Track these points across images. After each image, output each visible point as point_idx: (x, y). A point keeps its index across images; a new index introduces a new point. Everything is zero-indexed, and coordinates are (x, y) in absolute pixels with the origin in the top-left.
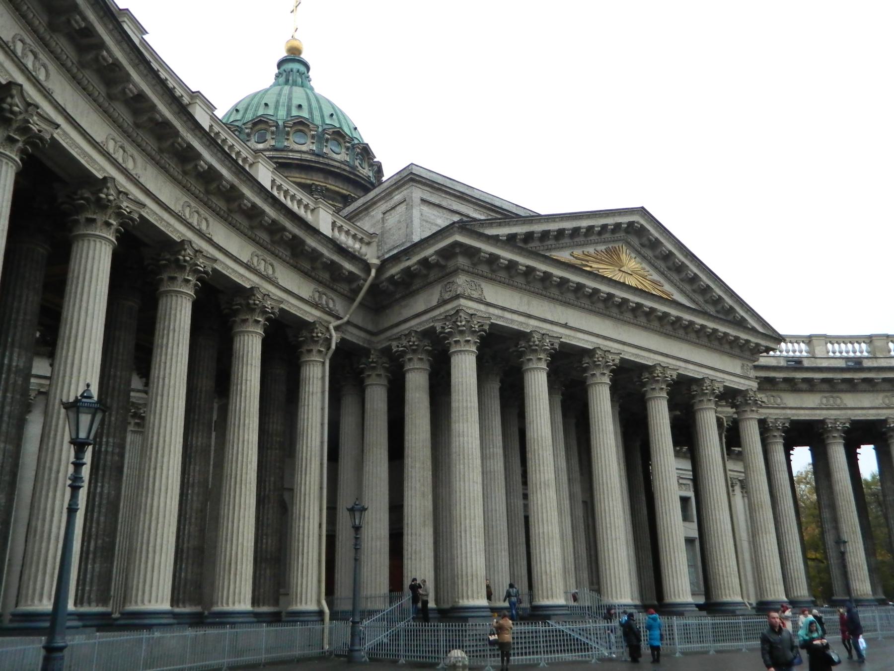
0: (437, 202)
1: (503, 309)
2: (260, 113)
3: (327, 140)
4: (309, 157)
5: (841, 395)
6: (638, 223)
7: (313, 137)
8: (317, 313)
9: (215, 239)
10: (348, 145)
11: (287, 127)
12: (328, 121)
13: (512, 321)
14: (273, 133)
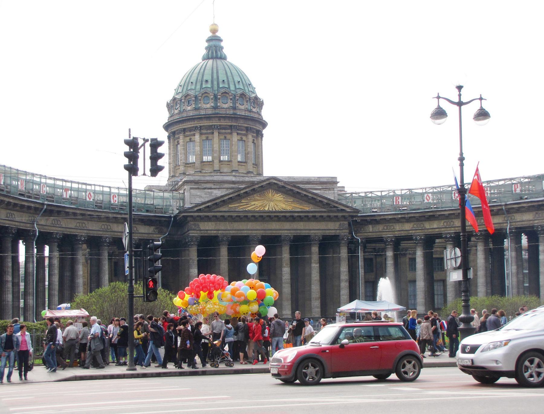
0: (197, 187)
1: (207, 230)
2: (189, 88)
3: (219, 99)
4: (210, 112)
5: (424, 223)
7: (212, 99)
8: (155, 235)
9: (114, 230)
10: (232, 97)
11: (200, 97)
12: (221, 86)
13: (211, 233)
14: (193, 101)
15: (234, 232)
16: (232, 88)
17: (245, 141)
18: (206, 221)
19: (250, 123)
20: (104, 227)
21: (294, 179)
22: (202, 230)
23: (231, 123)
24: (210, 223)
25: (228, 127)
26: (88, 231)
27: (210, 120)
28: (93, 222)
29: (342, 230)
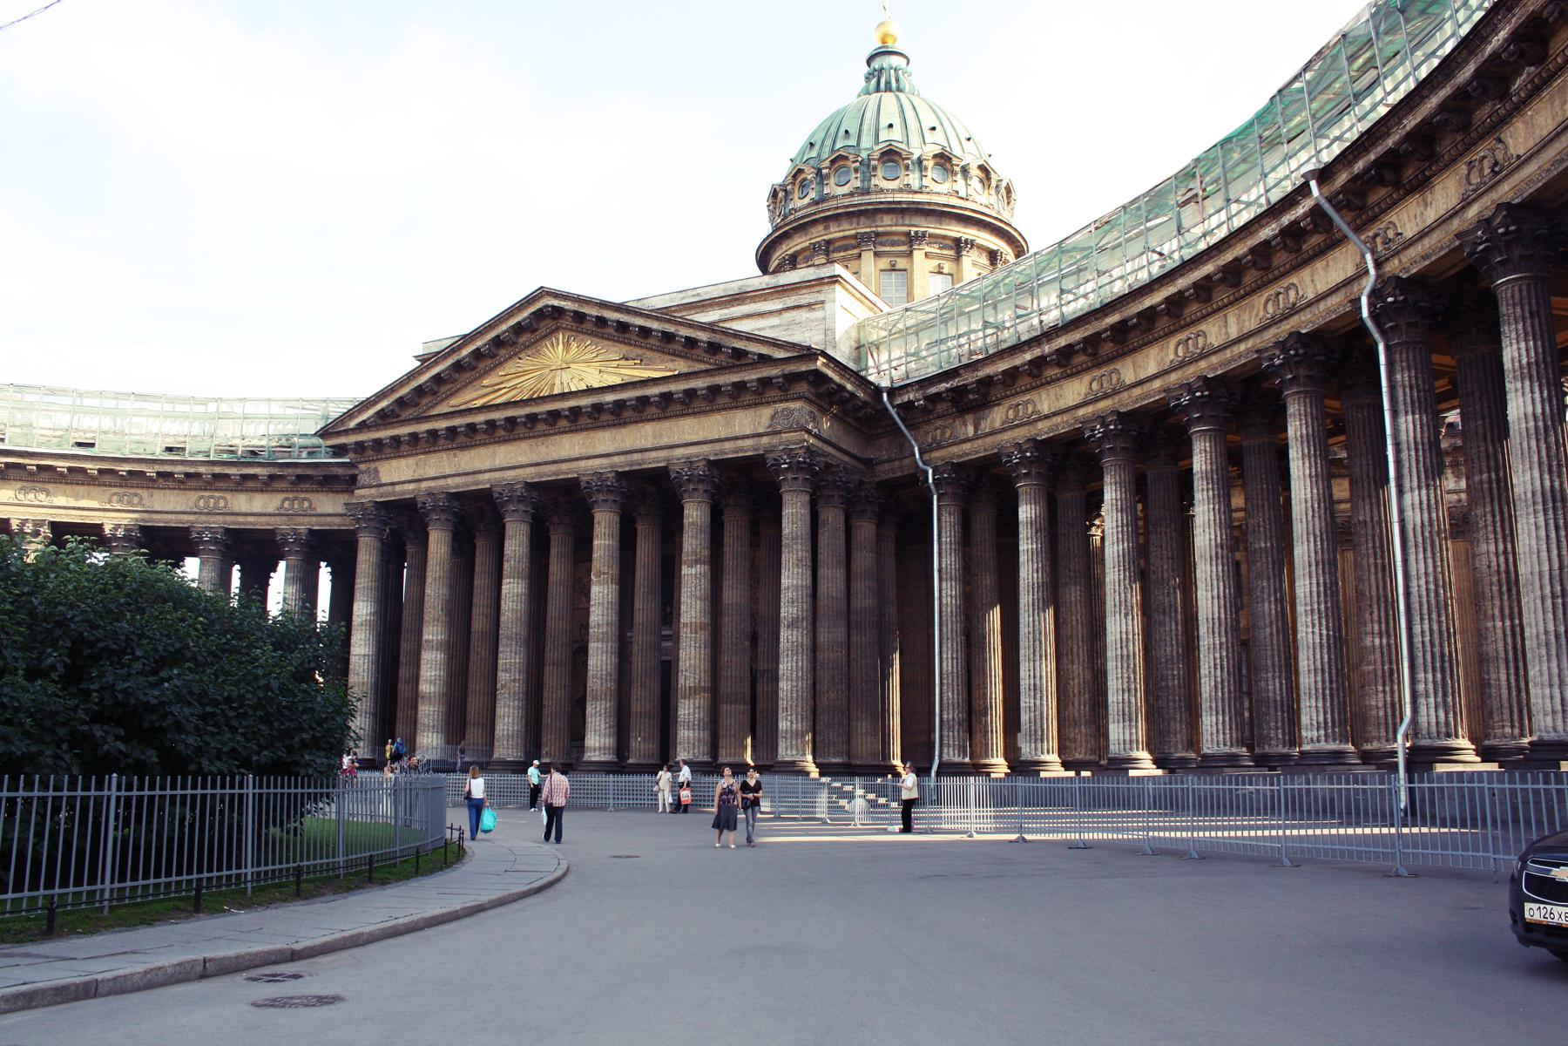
1: (392, 484)
3: (828, 176)
6: (547, 306)
9: (236, 509)
12: (838, 146)
13: (404, 492)
15: (457, 480)
16: (867, 142)
17: (905, 270)
18: (391, 458)
19: (917, 220)
20: (207, 503)
21: (698, 295)
22: (385, 485)
23: (854, 229)
24: (403, 462)
25: (853, 242)
26: (146, 516)
27: (806, 235)
28: (168, 491)
29: (780, 432)
